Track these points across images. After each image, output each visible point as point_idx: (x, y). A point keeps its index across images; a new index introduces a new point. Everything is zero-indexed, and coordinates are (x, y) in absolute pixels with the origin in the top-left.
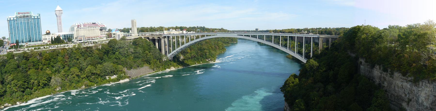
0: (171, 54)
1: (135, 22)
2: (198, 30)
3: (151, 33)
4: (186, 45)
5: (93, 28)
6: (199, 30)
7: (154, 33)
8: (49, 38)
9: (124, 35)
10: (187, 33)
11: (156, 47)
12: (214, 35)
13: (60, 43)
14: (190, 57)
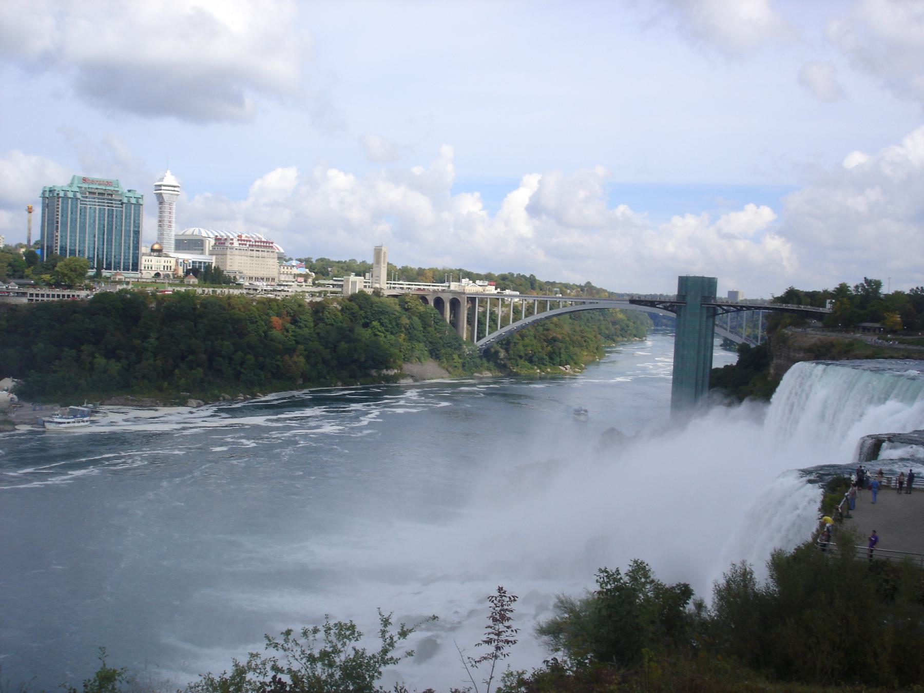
0: (496, 334)
1: (385, 253)
2: (555, 289)
3: (433, 286)
4: (512, 326)
5: (257, 252)
6: (558, 289)
7: (415, 285)
8: (169, 264)
9: (365, 284)
10: (498, 293)
11: (444, 320)
12: (594, 303)
13: (220, 283)
14: (522, 354)
